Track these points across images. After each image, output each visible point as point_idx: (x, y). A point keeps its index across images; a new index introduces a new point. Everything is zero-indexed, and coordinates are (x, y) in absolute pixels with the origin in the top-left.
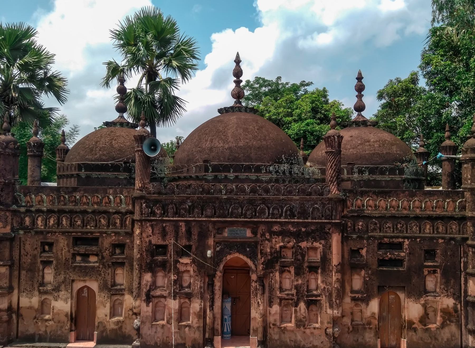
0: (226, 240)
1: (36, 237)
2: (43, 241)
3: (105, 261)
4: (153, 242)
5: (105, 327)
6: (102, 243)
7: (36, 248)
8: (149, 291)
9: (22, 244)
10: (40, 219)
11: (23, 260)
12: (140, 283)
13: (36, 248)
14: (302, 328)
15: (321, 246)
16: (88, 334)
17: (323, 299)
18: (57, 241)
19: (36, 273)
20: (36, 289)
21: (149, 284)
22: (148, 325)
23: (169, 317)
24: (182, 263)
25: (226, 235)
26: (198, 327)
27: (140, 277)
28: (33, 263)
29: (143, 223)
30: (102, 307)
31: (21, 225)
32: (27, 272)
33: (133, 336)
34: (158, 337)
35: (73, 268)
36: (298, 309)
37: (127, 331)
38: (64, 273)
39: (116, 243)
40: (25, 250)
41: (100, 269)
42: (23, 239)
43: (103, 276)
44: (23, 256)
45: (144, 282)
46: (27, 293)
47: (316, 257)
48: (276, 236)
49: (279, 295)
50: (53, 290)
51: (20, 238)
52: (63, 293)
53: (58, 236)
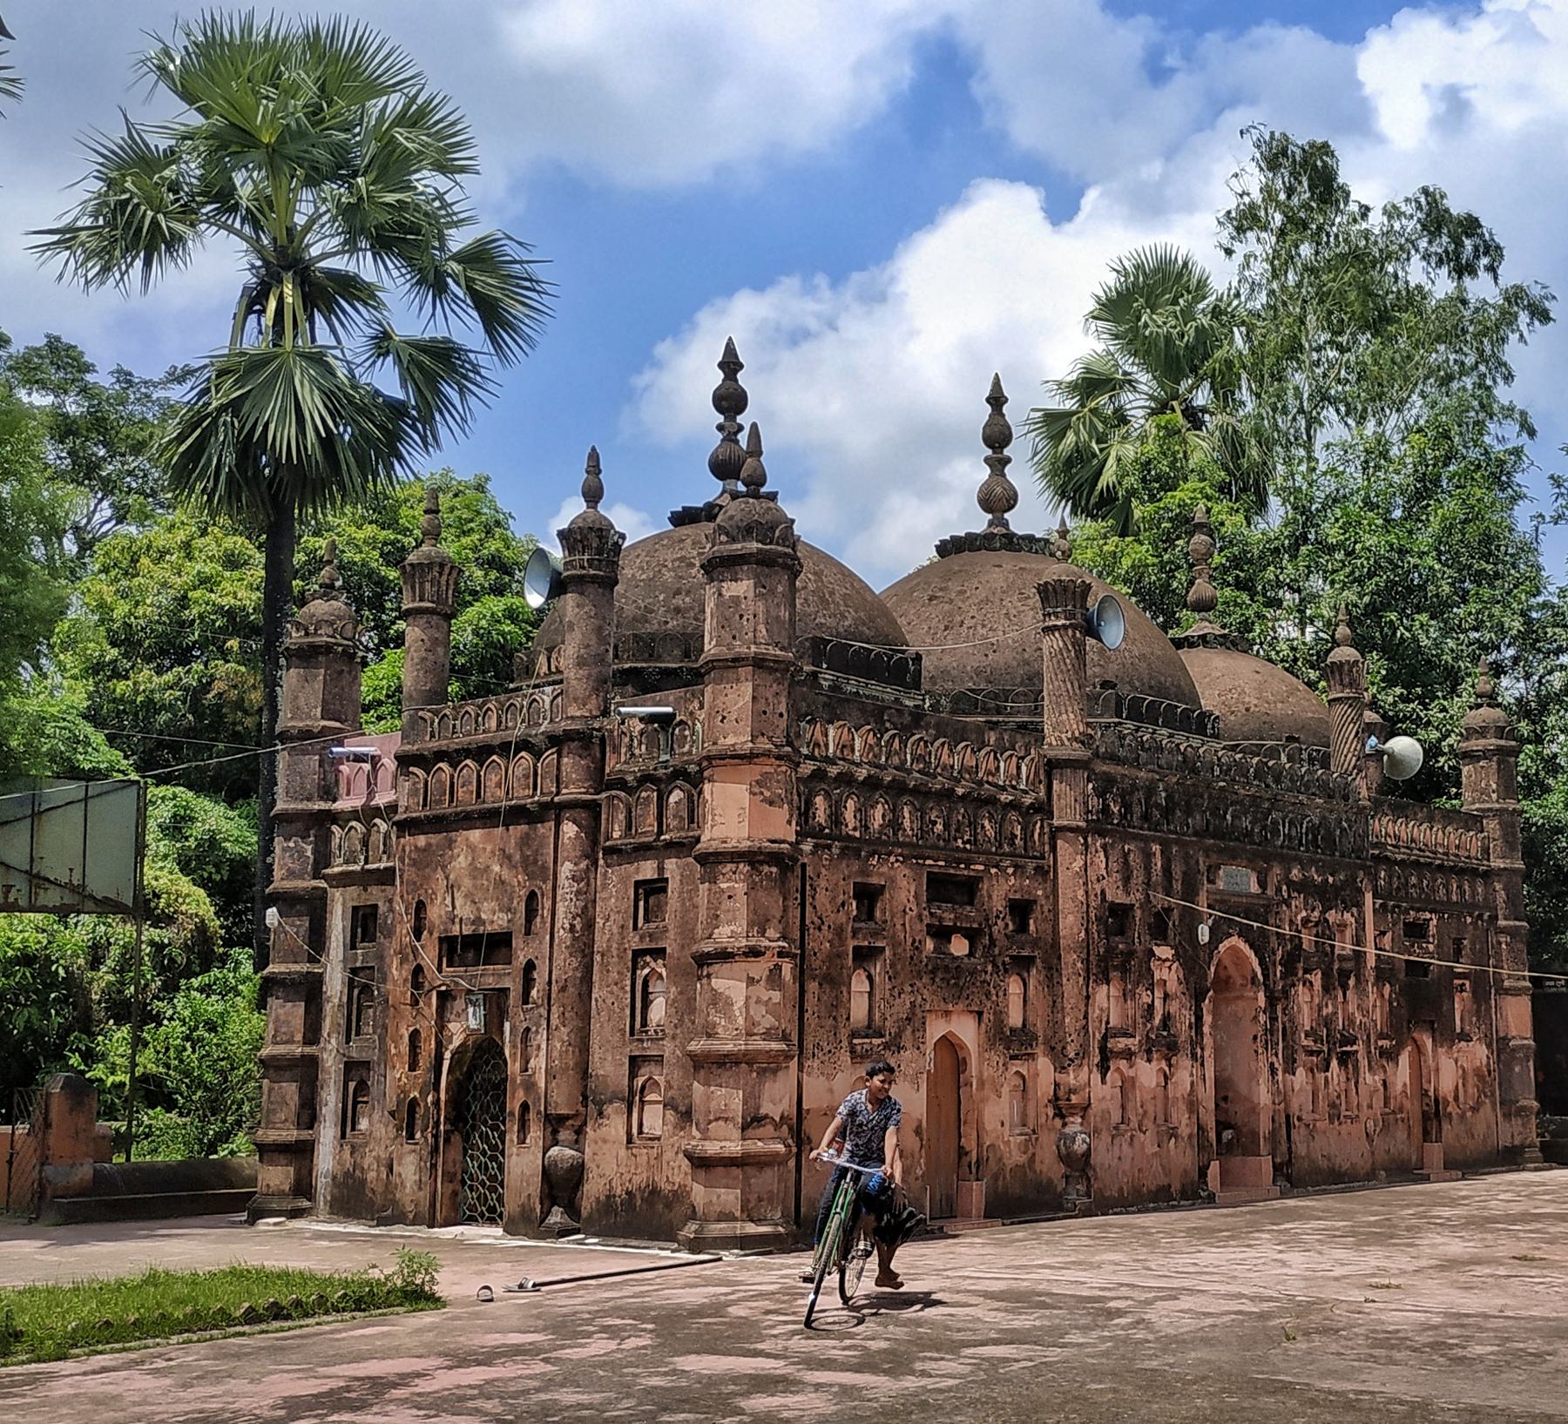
0: (1226, 898)
1: (844, 862)
2: (859, 880)
3: (997, 951)
4: (1109, 898)
5: (1000, 1159)
6: (990, 897)
7: (843, 904)
8: (1105, 1038)
9: (808, 888)
10: (850, 804)
11: (811, 945)
12: (1086, 1017)
13: (843, 904)
14: (1336, 1123)
15: (1353, 920)
16: (938, 1197)
17: (1359, 1047)
18: (893, 880)
19: (844, 989)
20: (845, 1044)
21: (1105, 1019)
22: (1106, 1137)
23: (1141, 1111)
24: (1160, 959)
25: (1221, 885)
26: (1190, 1136)
27: (1088, 997)
28: (836, 956)
29: (1089, 839)
30: (993, 1096)
31: (806, 822)
32: (820, 984)
33: (1056, 1181)
34: (1124, 1172)
35: (932, 972)
36: (1329, 1074)
37: (1045, 1170)
38: (910, 989)
39: (1018, 896)
40: (815, 907)
41: (988, 978)
42: (809, 871)
43: (994, 998)
44: (811, 931)
45: (1094, 1013)
46: (823, 1058)
47: (1344, 946)
48: (1296, 894)
49: (1305, 1043)
50: (887, 1046)
51: (804, 866)
52: (905, 1055)
53: (896, 865)
